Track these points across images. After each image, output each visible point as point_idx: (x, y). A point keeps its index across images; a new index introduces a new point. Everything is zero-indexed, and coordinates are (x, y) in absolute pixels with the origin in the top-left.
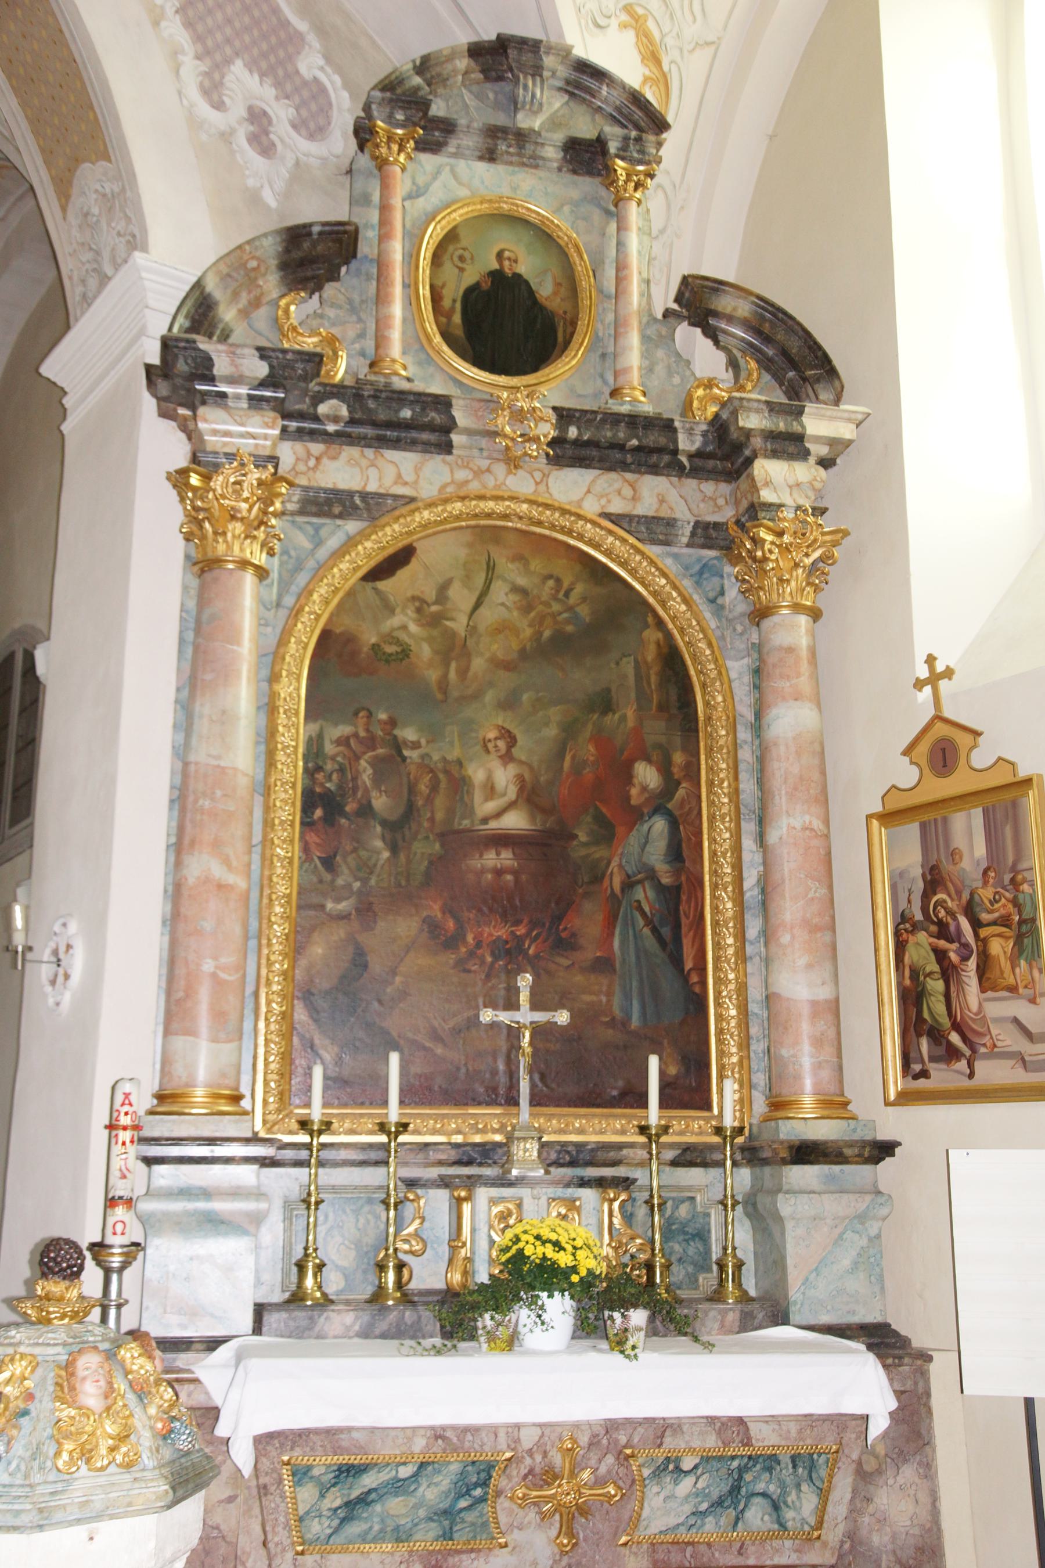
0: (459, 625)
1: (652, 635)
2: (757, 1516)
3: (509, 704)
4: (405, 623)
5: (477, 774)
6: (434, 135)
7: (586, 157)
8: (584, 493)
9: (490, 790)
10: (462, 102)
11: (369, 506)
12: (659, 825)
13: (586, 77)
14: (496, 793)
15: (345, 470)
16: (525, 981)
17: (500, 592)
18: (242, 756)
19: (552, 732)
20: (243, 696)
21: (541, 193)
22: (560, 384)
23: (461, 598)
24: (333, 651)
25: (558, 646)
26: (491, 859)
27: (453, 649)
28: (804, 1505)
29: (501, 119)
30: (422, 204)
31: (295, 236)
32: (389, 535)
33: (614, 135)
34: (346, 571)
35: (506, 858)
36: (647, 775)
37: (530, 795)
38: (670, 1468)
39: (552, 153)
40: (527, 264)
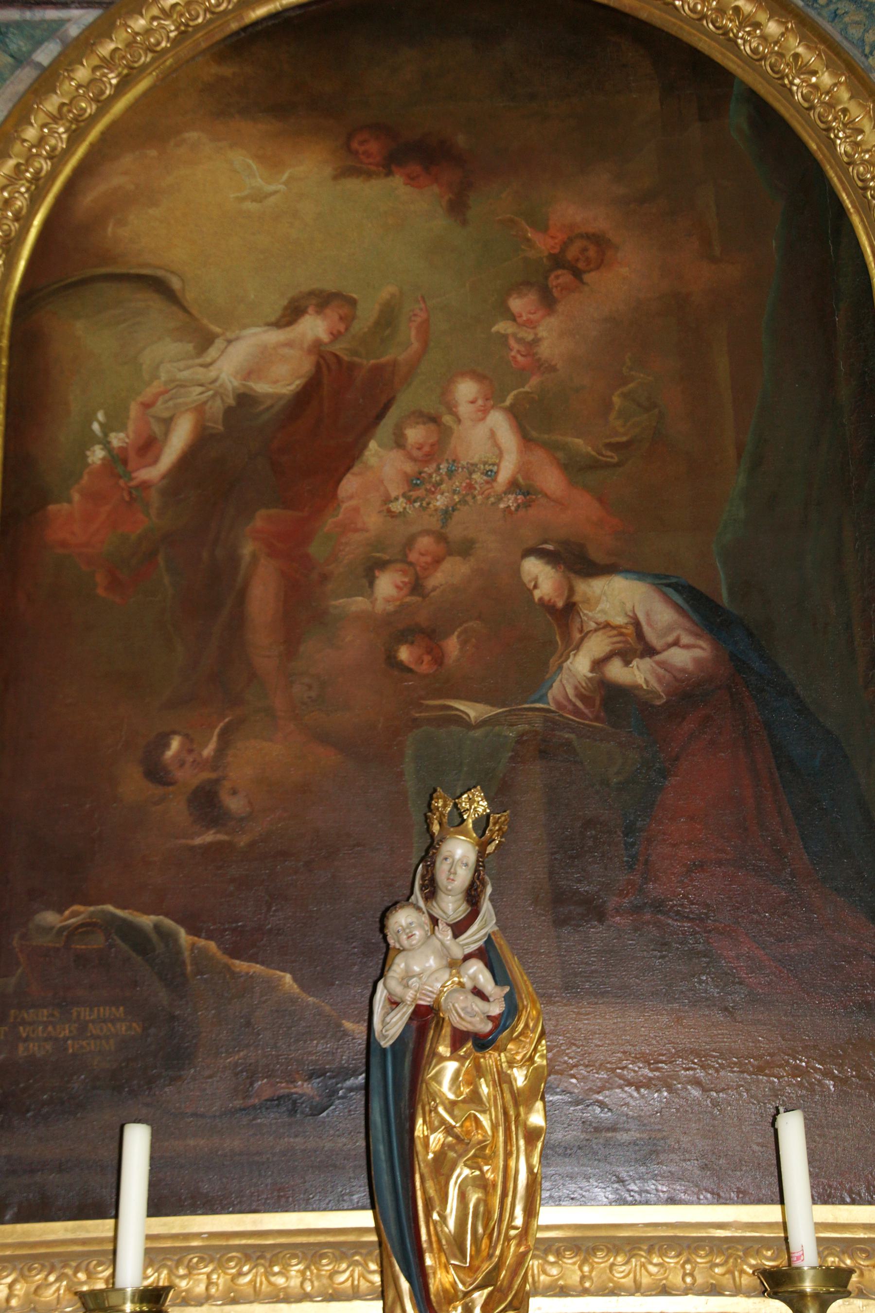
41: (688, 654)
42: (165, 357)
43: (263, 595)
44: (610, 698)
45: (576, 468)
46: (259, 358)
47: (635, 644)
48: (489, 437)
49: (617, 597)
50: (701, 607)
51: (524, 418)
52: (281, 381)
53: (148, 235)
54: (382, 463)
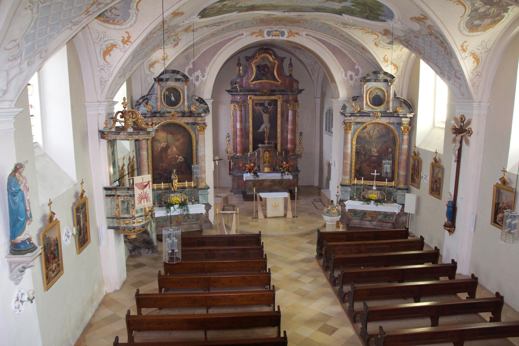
0: (371, 134)
1: (392, 135)
2: (387, 218)
3: (376, 142)
4: (366, 134)
5: (373, 150)
6: (369, 81)
7: (386, 81)
8: (384, 121)
9: (374, 151)
10: (372, 77)
11: (362, 123)
12: (391, 155)
13: (386, 73)
14: (374, 151)
15: (359, 120)
16: (375, 171)
17: (376, 131)
18: (349, 151)
19: (380, 145)
20: (349, 146)
21: (381, 85)
22: (382, 108)
23: (372, 132)
24: (358, 137)
25: (382, 136)
26: (374, 158)
27: (371, 137)
28: (391, 218)
29: (376, 78)
30: (368, 88)
31: (353, 97)
32: (364, 125)
33: (389, 79)
34: (359, 130)
35: (375, 158)
36: (390, 150)
37: (378, 152)
38: (380, 214)
39: (382, 81)
40: (380, 93)
41: (183, 160)
42: (159, 145)
43: (164, 157)
44: (180, 162)
45: (179, 151)
46: (163, 145)
47: (181, 159)
48: (175, 149)
49: (180, 157)
50: (184, 157)
51: (176, 148)
52: (164, 146)
53: (158, 138)
54: (169, 150)
